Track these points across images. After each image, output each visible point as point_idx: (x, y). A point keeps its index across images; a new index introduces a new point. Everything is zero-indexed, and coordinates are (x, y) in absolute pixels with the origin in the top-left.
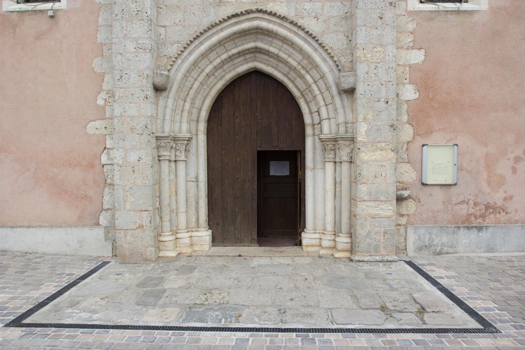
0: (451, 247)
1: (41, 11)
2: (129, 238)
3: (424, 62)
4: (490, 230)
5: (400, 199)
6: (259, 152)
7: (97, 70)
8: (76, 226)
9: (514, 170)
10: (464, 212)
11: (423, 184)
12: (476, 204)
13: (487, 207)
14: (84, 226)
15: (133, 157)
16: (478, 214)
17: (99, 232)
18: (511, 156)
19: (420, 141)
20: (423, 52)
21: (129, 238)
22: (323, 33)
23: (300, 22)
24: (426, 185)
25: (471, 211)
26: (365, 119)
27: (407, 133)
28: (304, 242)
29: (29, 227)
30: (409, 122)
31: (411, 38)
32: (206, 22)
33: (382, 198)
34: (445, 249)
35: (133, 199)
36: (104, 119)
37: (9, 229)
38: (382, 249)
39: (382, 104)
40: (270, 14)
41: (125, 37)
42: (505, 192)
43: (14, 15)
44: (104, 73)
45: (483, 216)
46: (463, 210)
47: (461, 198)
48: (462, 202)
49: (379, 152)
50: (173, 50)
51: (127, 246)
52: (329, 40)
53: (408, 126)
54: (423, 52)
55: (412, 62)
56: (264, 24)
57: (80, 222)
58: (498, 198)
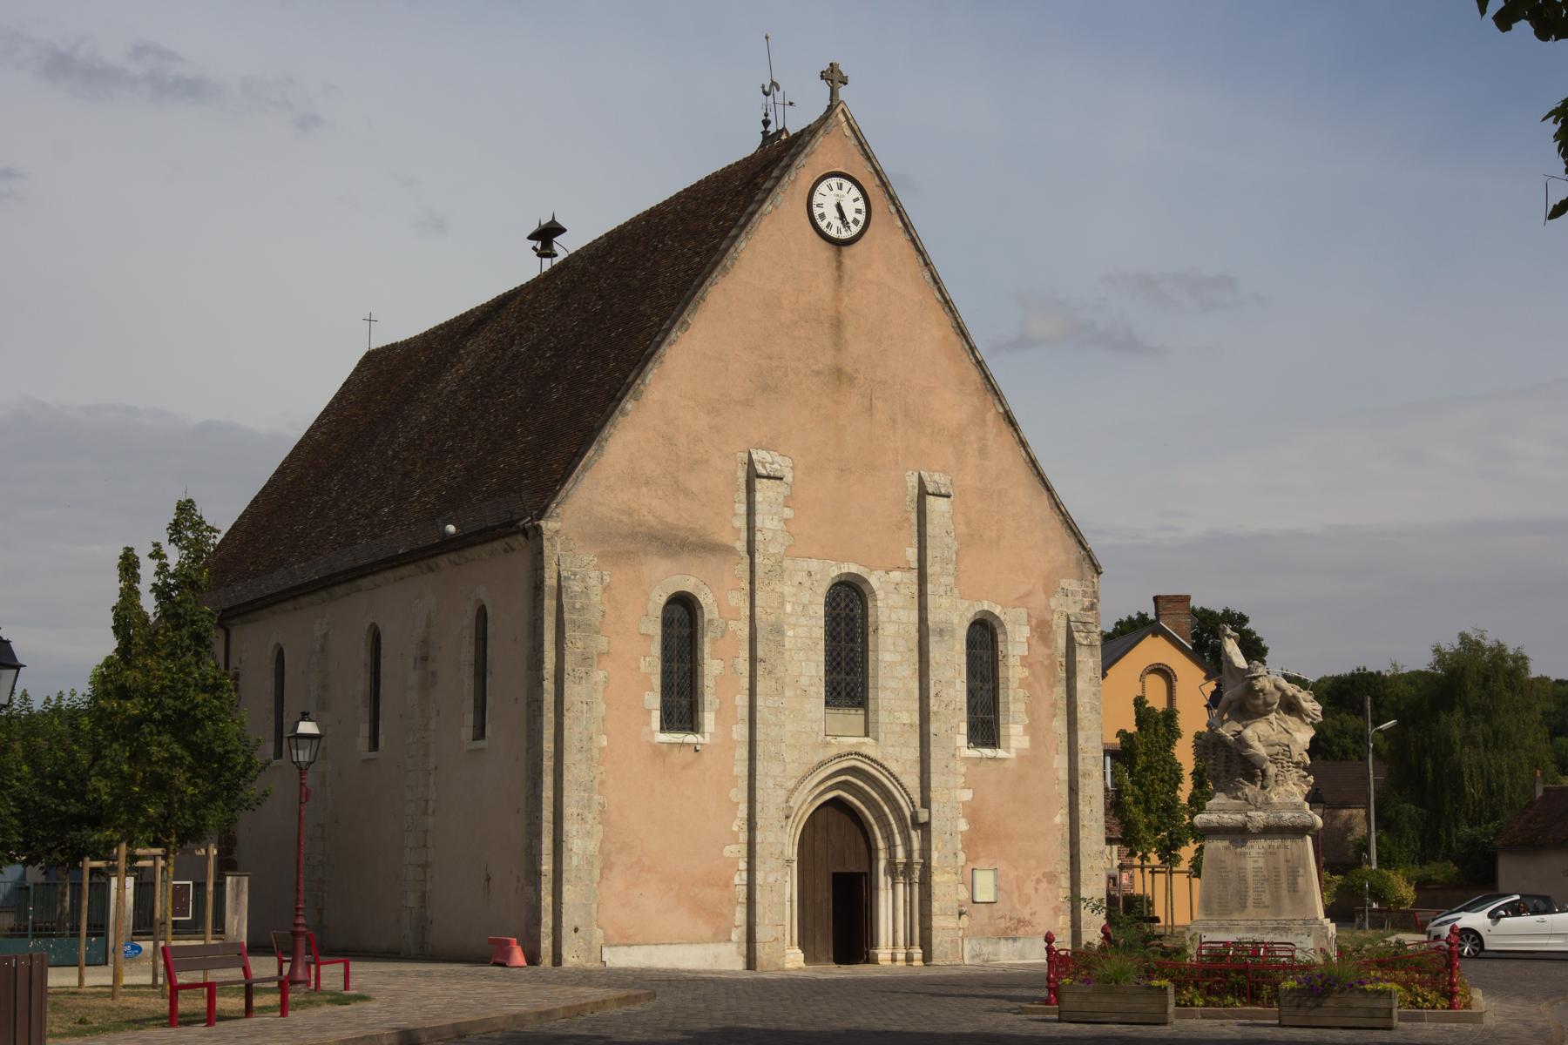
0: (995, 955)
1: (689, 744)
2: (767, 950)
3: (973, 799)
4: (1022, 940)
5: (961, 914)
6: (834, 874)
7: (734, 799)
8: (713, 942)
9: (1036, 890)
10: (1003, 926)
11: (974, 902)
12: (1011, 919)
13: (1019, 921)
14: (719, 942)
15: (771, 879)
16: (1013, 927)
17: (732, 947)
18: (1034, 878)
19: (971, 866)
20: (971, 790)
21: (767, 950)
22: (902, 773)
23: (886, 764)
24: (976, 903)
25: (1008, 924)
26: (937, 848)
27: (962, 857)
28: (880, 957)
29: (671, 944)
30: (962, 850)
31: (963, 780)
32: (816, 760)
33: (949, 913)
34: (991, 957)
35: (771, 915)
36: (737, 843)
37: (654, 946)
38: (950, 956)
39: (948, 836)
40: (866, 757)
41: (766, 775)
42: (1031, 908)
43: (665, 746)
44: (739, 803)
45: (1016, 929)
46: (1003, 924)
47: (1000, 914)
48: (1002, 917)
49: (946, 875)
50: (791, 784)
51: (764, 957)
52: (904, 779)
53: (962, 852)
54: (971, 790)
55: (964, 799)
56: (859, 764)
57: (715, 939)
58: (1026, 914)
